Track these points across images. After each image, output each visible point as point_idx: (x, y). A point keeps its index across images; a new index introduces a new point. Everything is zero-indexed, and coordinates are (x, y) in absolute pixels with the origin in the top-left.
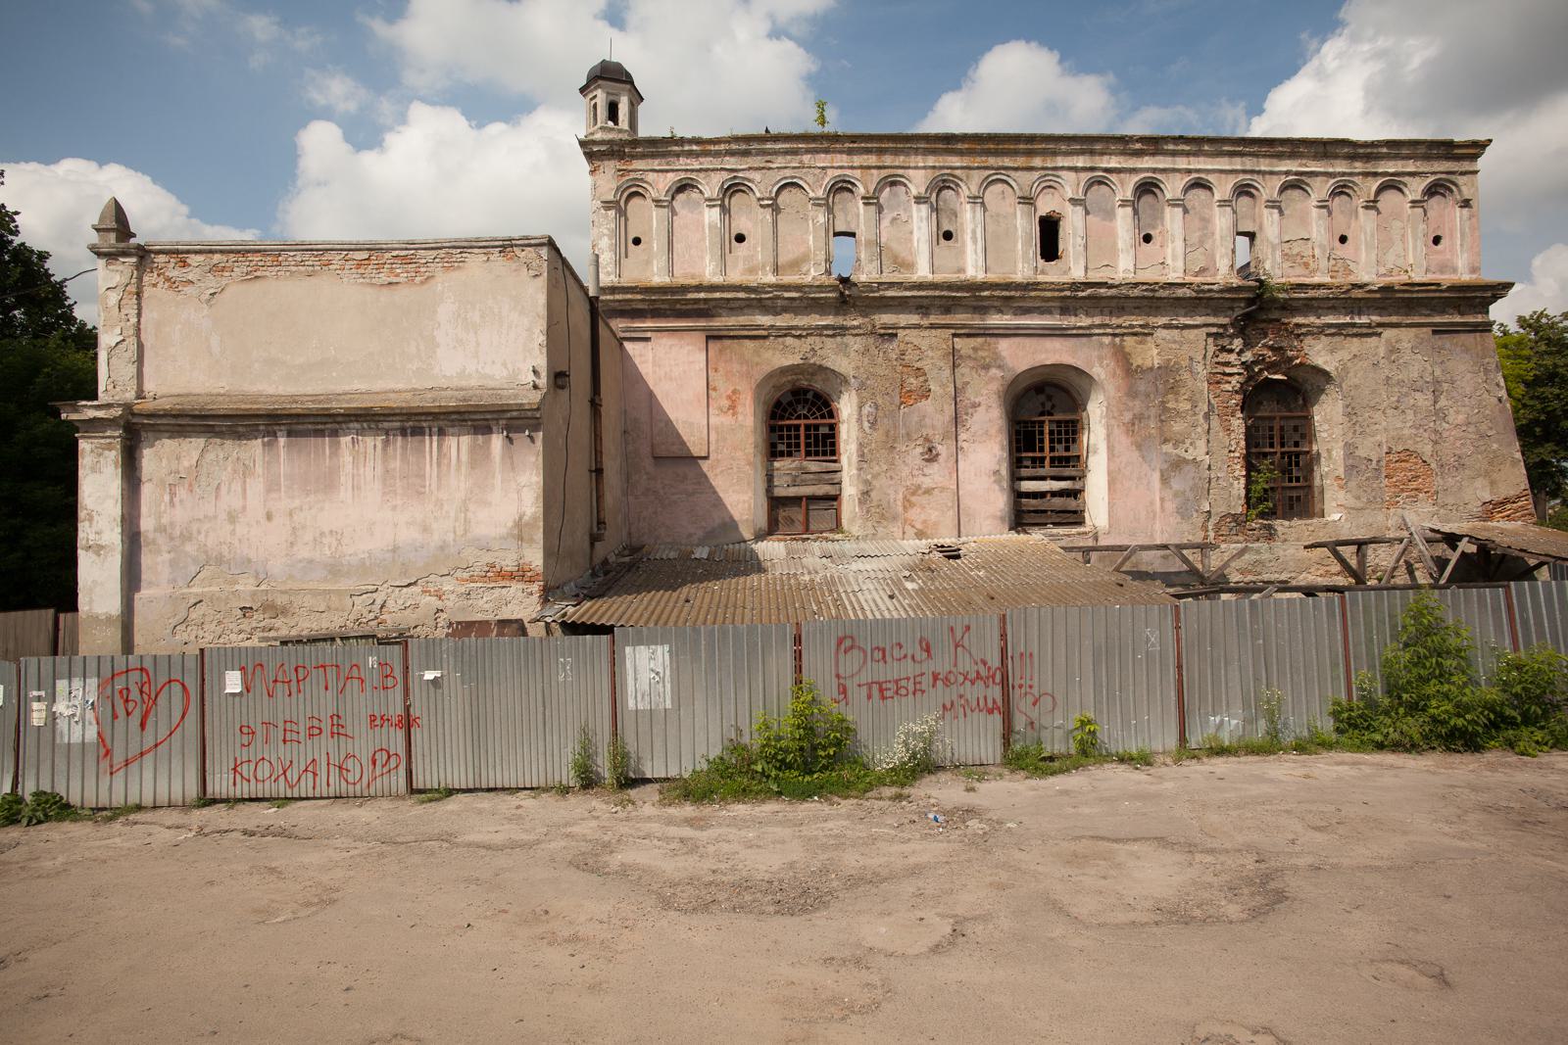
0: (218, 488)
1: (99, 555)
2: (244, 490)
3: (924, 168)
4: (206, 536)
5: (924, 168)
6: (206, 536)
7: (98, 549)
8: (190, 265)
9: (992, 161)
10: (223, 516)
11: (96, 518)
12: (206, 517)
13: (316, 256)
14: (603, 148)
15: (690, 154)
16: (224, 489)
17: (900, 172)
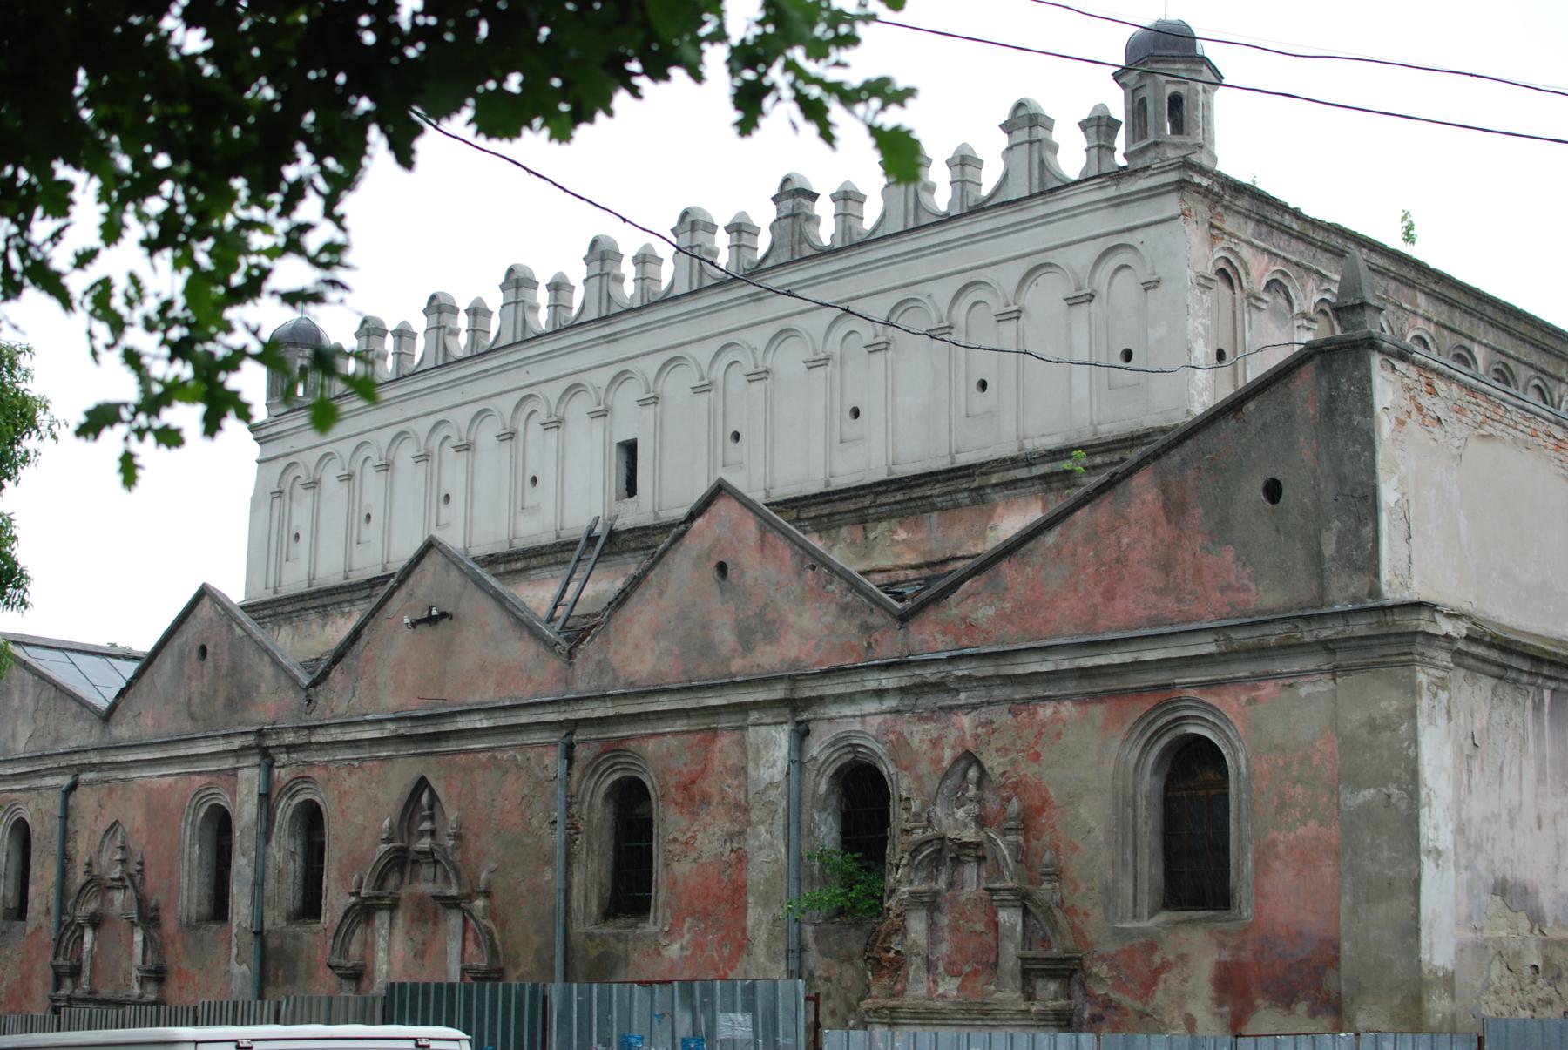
0: (1501, 769)
1: (1438, 866)
2: (1521, 775)
3: (1486, 345)
4: (1493, 846)
5: (1486, 345)
6: (1493, 846)
7: (1438, 854)
8: (1436, 393)
9: (1535, 357)
10: (1505, 817)
11: (1434, 802)
12: (1493, 813)
13: (1527, 419)
14: (1205, 182)
15: (1287, 231)
16: (1506, 770)
17: (1467, 343)
